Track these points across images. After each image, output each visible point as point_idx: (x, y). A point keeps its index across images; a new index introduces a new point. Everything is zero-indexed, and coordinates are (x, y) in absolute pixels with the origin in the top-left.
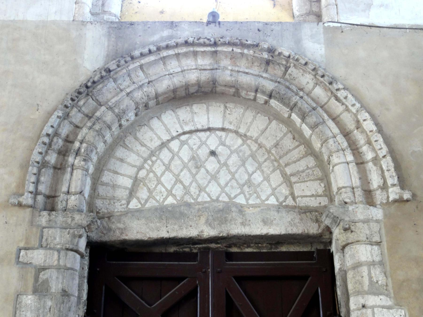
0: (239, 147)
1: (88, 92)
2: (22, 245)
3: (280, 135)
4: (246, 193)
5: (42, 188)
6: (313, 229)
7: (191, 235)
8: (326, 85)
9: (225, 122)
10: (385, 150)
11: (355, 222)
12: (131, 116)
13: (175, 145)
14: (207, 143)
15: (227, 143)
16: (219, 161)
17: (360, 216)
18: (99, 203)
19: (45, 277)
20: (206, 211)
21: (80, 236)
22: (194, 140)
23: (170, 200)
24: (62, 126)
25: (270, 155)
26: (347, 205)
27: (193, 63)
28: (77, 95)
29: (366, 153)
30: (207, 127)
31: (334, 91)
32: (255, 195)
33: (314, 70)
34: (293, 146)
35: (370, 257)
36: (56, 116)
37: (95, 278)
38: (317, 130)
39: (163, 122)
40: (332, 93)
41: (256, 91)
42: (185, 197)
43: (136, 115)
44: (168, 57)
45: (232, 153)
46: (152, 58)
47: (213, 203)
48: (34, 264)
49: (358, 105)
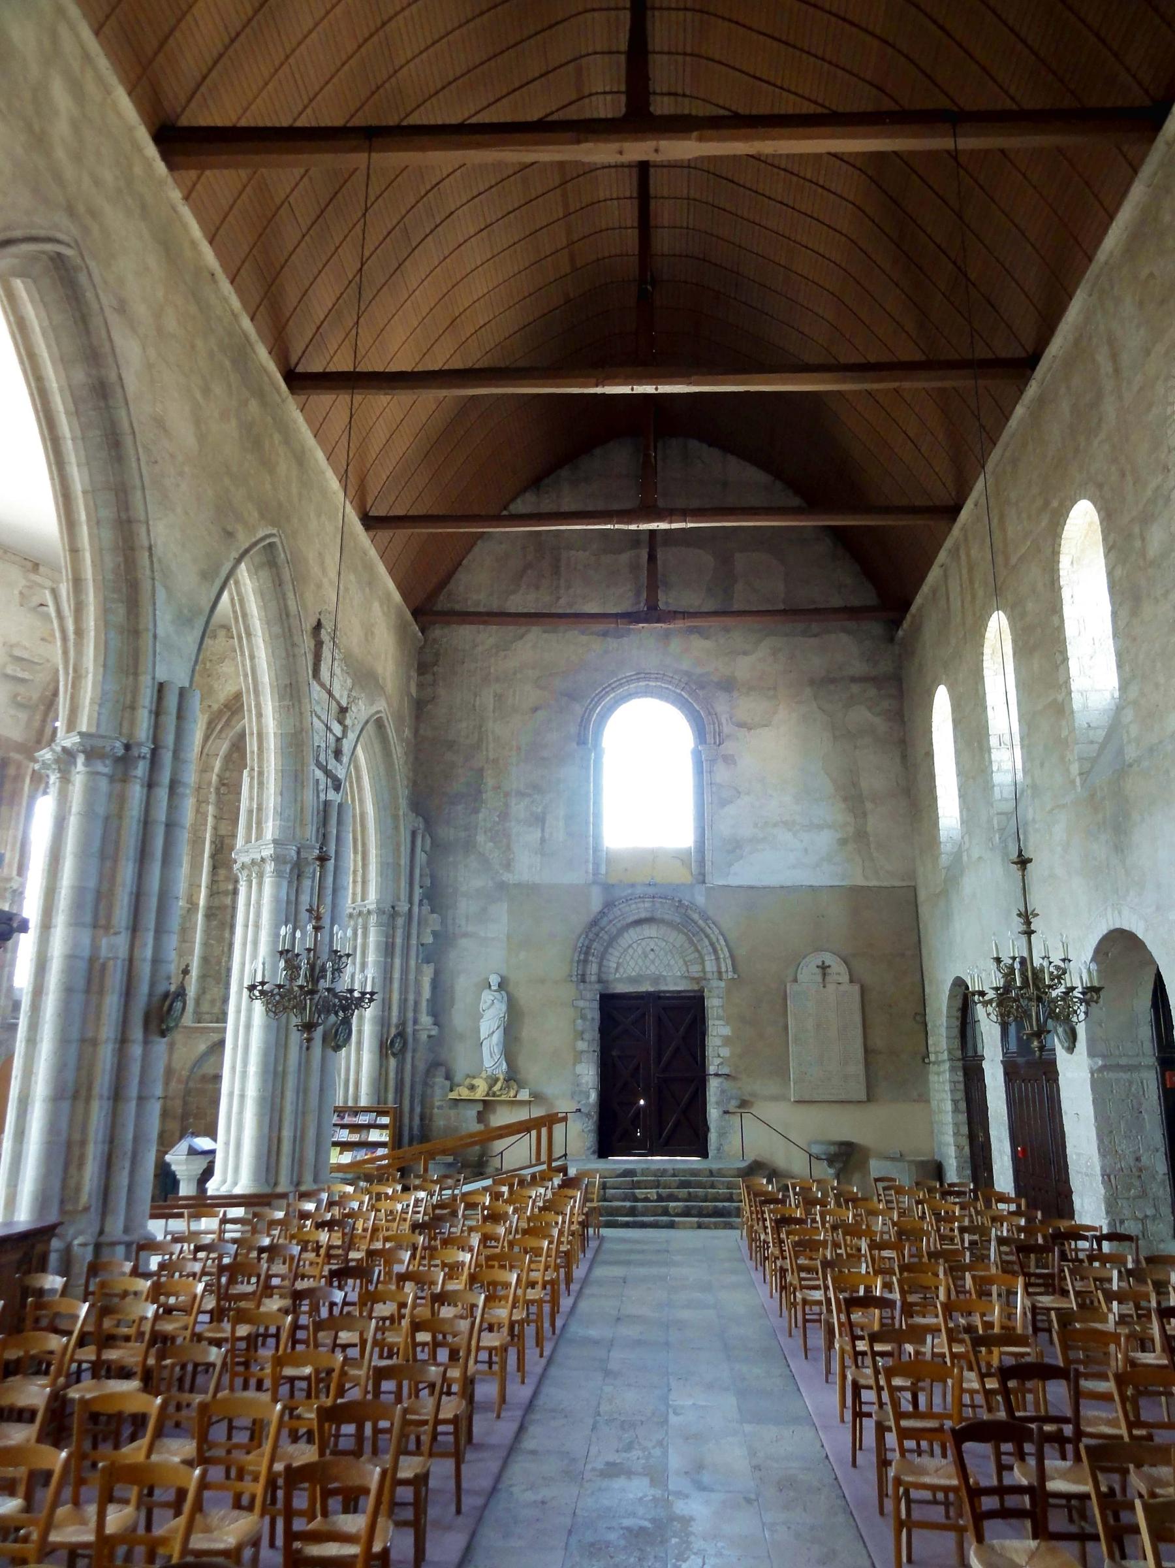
6: (696, 988)
10: (727, 955)
18: (604, 977)
22: (644, 943)
23: (634, 974)
37: (602, 1009)
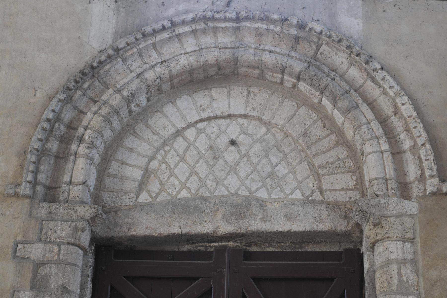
0: (262, 136)
1: (93, 73)
2: (19, 238)
3: (308, 123)
4: (269, 187)
5: (42, 177)
6: (342, 226)
7: (205, 232)
8: (361, 65)
9: (248, 108)
11: (387, 217)
12: (142, 100)
13: (190, 133)
14: (227, 131)
15: (250, 132)
16: (239, 152)
17: (393, 210)
18: (105, 196)
19: (44, 273)
20: (223, 206)
21: (83, 230)
22: (212, 128)
23: (184, 194)
24: (64, 110)
25: (298, 145)
26: (379, 198)
27: (213, 41)
28: (81, 76)
29: (403, 142)
30: (227, 113)
31: (371, 72)
32: (279, 189)
33: (348, 47)
34: (323, 135)
35: (401, 255)
36: (57, 100)
38: (350, 115)
39: (178, 109)
40: (368, 73)
41: (283, 72)
42: (201, 190)
43: (148, 100)
44: (185, 34)
45: (254, 142)
46: (166, 35)
47: (231, 197)
48: (32, 259)
49: (397, 88)
